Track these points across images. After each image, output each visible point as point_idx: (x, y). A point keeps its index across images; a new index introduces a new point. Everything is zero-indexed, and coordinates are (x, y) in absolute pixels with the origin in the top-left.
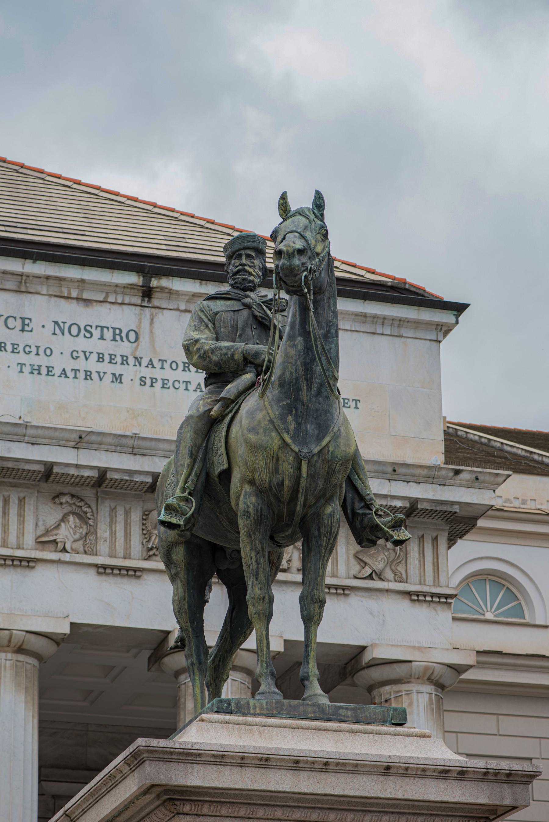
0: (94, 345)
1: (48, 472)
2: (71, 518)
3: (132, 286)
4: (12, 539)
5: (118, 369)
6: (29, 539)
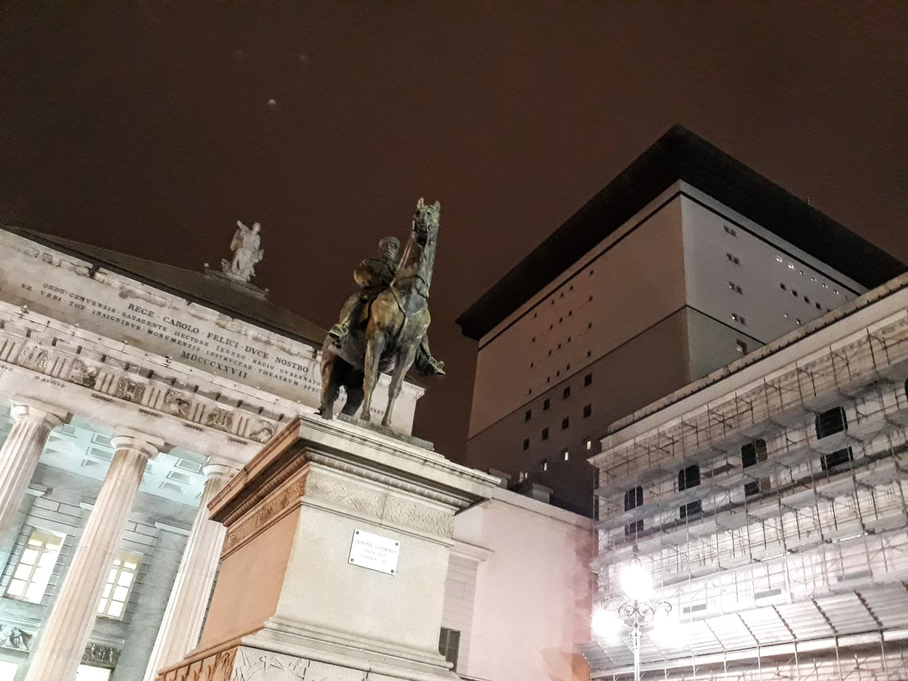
0: (290, 369)
1: (261, 410)
4: (241, 433)
6: (247, 434)
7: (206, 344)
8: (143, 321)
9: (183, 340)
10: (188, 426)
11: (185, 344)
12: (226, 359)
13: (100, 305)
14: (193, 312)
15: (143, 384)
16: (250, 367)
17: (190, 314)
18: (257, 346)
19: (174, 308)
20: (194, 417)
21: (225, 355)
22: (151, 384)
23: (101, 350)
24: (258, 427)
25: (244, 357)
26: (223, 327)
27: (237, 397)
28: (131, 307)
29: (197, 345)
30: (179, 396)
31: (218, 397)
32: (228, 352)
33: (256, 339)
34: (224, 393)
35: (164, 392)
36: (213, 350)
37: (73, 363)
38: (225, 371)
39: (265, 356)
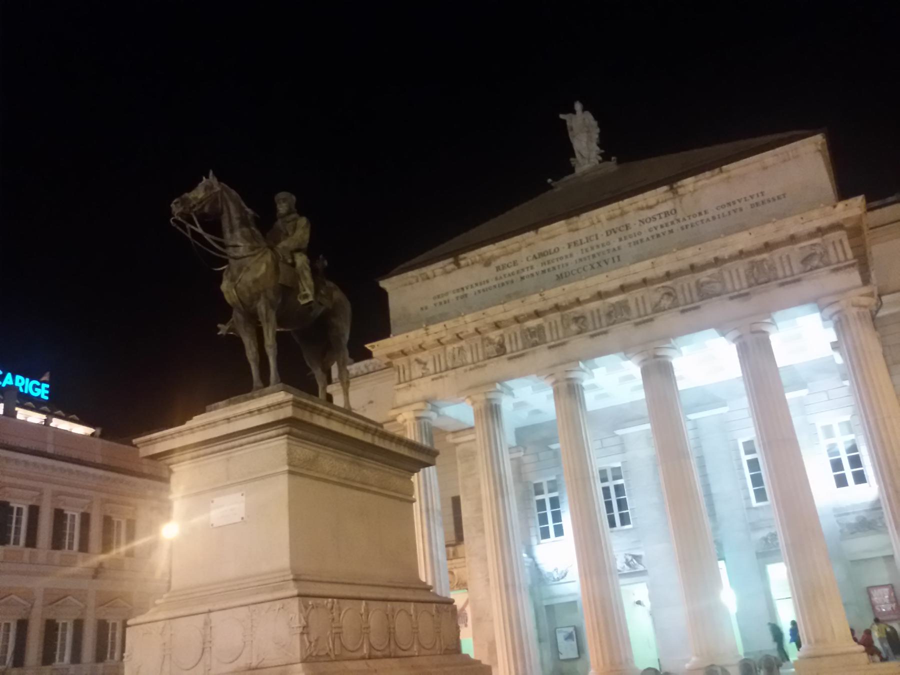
1: (645, 282)
2: (666, 297)
3: (666, 191)
4: (642, 313)
5: (671, 227)
6: (649, 310)
7: (571, 255)
8: (513, 274)
9: (552, 265)
10: (592, 336)
11: (554, 268)
12: (594, 256)
13: (476, 285)
14: (545, 236)
15: (539, 325)
16: (619, 248)
17: (544, 240)
18: (615, 224)
19: (530, 245)
20: (594, 324)
21: (591, 253)
22: (546, 321)
23: (489, 320)
24: (656, 297)
25: (608, 243)
26: (577, 230)
27: (616, 284)
28: (498, 269)
29: (564, 261)
30: (573, 315)
31: (600, 295)
32: (592, 248)
33: (610, 218)
34: (602, 288)
35: (559, 319)
36: (581, 256)
37: (482, 343)
38: (599, 265)
39: (627, 227)
